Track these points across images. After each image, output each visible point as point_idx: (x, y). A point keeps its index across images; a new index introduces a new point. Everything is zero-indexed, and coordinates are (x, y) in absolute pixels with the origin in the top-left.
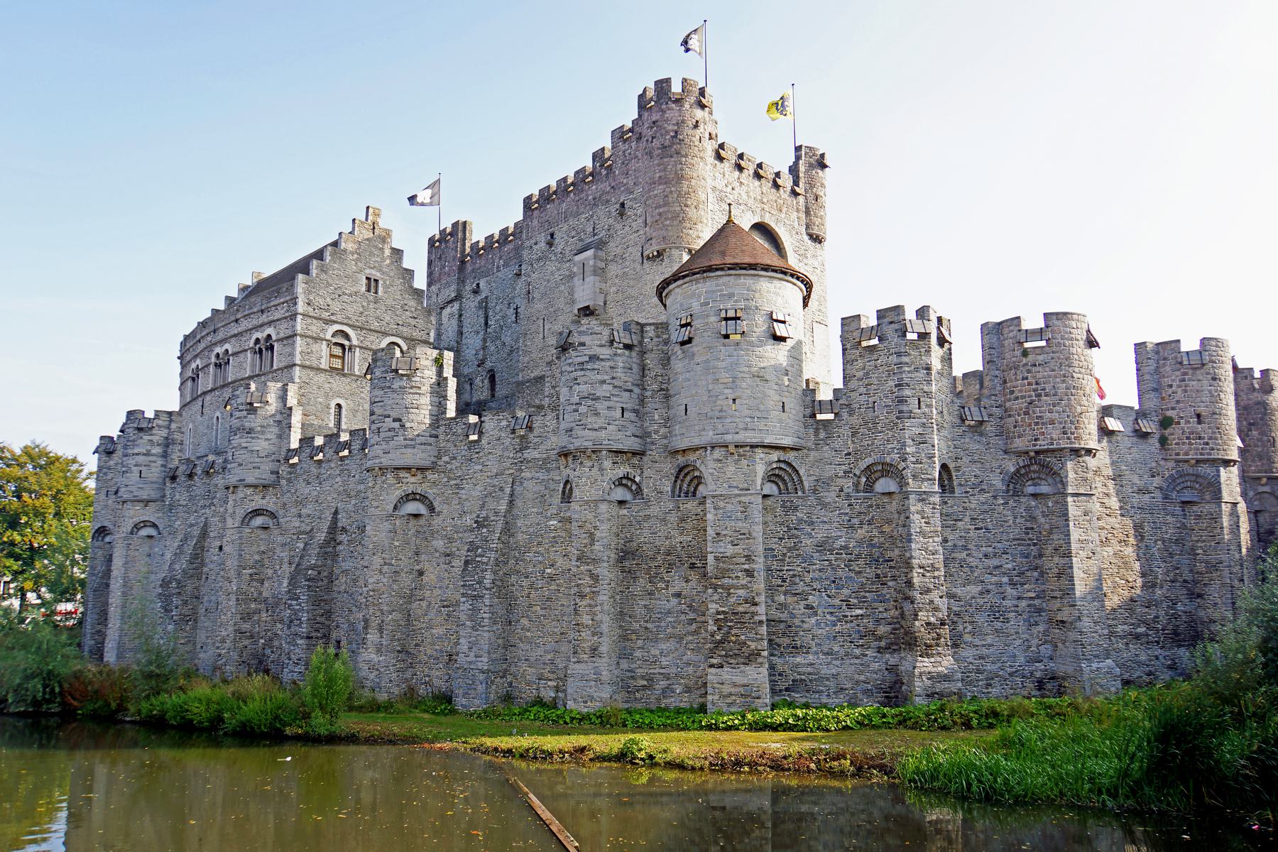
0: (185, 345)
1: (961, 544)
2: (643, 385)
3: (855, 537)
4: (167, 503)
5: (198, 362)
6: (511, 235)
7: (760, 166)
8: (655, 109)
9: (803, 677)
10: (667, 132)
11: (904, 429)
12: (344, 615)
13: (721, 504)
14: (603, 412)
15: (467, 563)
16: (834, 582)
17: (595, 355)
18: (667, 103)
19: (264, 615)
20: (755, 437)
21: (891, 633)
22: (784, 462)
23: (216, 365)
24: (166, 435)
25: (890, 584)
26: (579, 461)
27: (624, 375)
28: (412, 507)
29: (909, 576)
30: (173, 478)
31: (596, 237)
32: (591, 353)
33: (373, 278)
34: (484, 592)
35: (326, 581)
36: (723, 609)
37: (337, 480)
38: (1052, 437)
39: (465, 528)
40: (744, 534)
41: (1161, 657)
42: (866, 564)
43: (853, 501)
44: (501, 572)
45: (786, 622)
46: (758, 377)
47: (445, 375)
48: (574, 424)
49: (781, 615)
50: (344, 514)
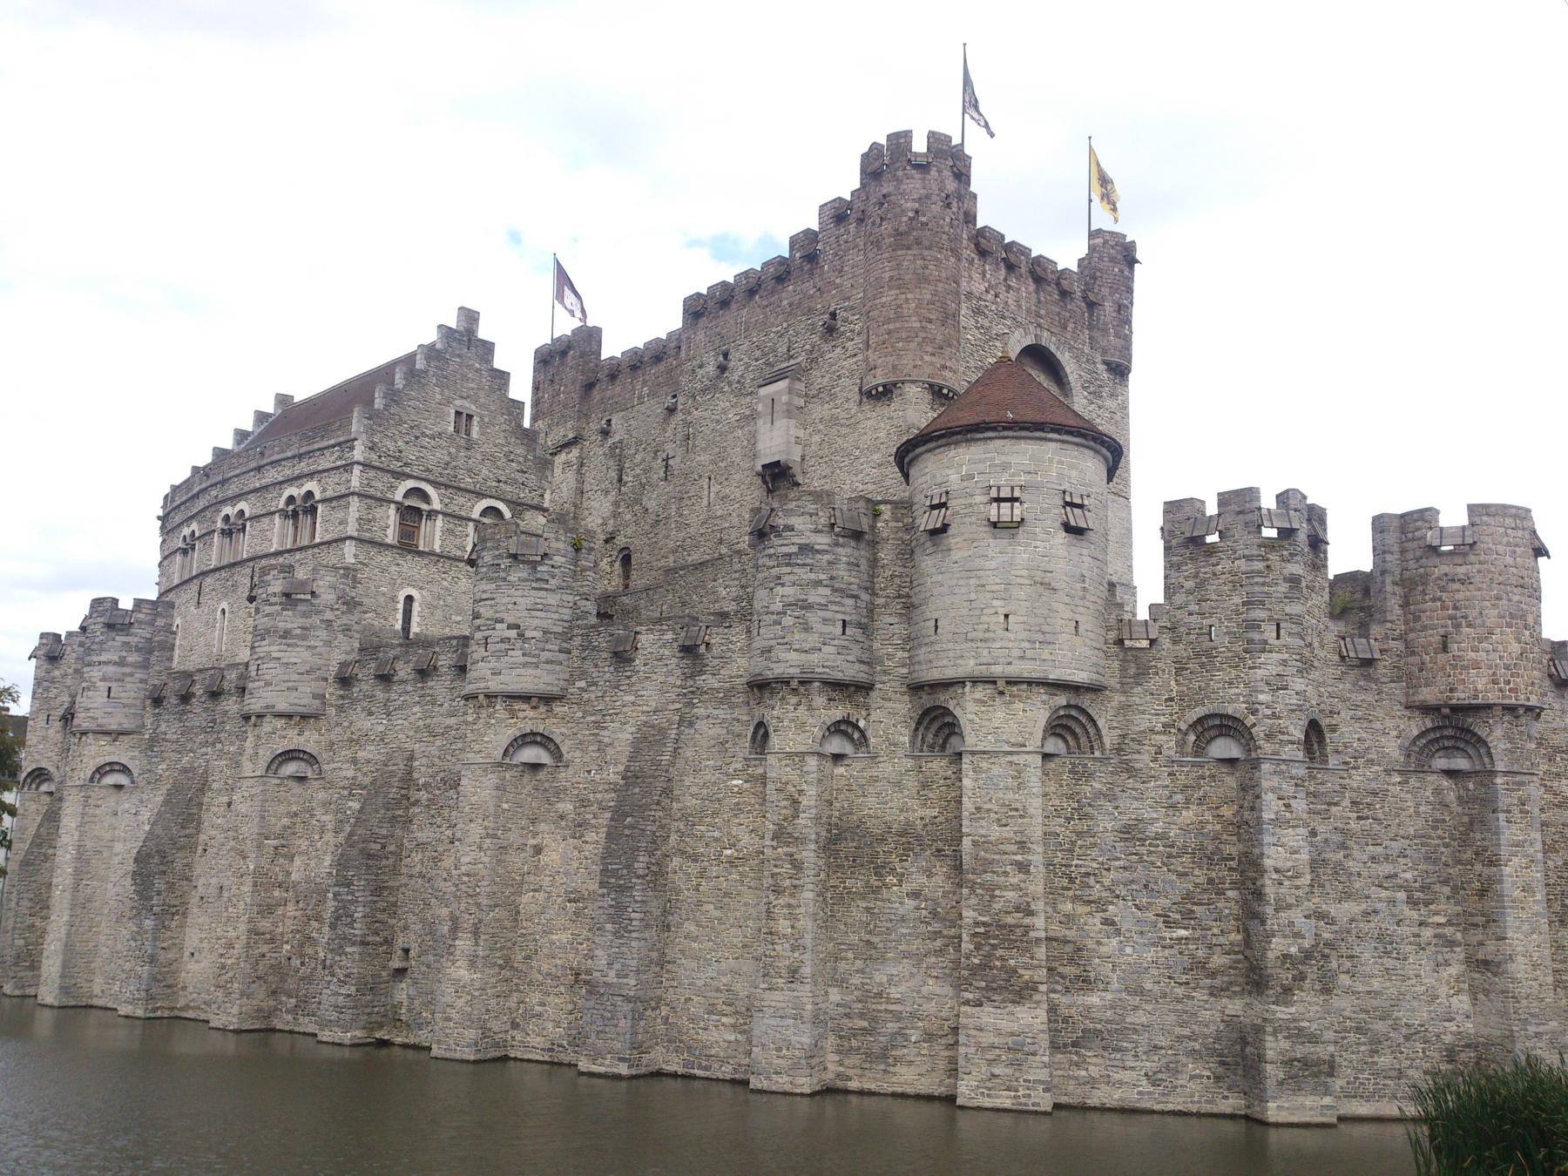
0: (173, 501)
1: (1337, 838)
2: (873, 589)
3: (1179, 821)
4: (147, 736)
5: (194, 526)
8: (887, 176)
9: (1099, 1026)
11: (1255, 668)
12: (417, 911)
13: (984, 765)
14: (818, 627)
15: (609, 836)
16: (1146, 886)
17: (807, 545)
18: (905, 169)
19: (291, 907)
20: (1035, 670)
21: (1230, 968)
22: (1076, 707)
23: (223, 532)
24: (149, 636)
25: (1230, 893)
28: (530, 754)
29: (1258, 883)
30: (157, 701)
31: (792, 362)
32: (803, 541)
33: (465, 412)
34: (633, 880)
35: (391, 861)
36: (984, 919)
37: (415, 710)
38: (1477, 686)
39: (607, 787)
40: (1017, 810)
42: (1193, 862)
43: (1176, 768)
45: (1075, 943)
46: (1042, 584)
49: (1067, 932)
50: (424, 761)
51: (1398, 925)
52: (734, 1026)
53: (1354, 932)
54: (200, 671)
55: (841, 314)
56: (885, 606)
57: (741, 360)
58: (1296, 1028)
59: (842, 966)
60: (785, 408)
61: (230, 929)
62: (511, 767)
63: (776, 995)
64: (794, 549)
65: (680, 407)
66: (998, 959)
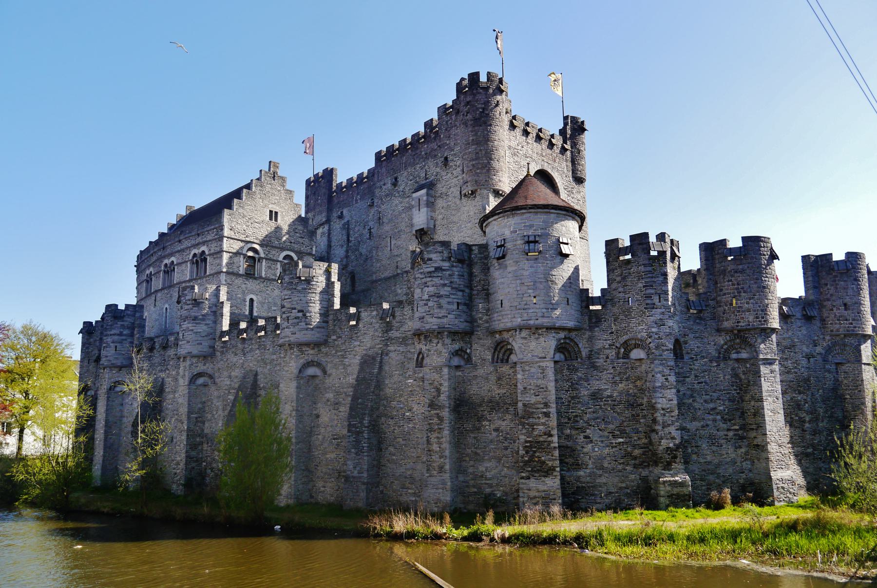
0: (141, 258)
1: (689, 393)
5: (151, 269)
6: (365, 178)
7: (540, 130)
9: (584, 485)
10: (478, 109)
11: (650, 316)
13: (527, 368)
14: (445, 306)
15: (351, 408)
17: (439, 267)
18: (477, 89)
20: (549, 322)
21: (643, 454)
22: (569, 338)
23: (164, 271)
25: (641, 421)
26: (429, 339)
27: (458, 280)
28: (311, 371)
29: (655, 416)
32: (436, 265)
34: (363, 429)
36: (528, 439)
37: (256, 352)
40: (543, 388)
41: (823, 469)
42: (625, 408)
44: (375, 416)
45: (571, 447)
47: (333, 280)
48: (425, 314)
50: (262, 376)
51: (718, 431)
52: (414, 493)
53: (698, 435)
54: (157, 337)
55: (450, 158)
56: (477, 295)
57: (403, 181)
58: (673, 481)
59: (464, 464)
60: (425, 202)
61: (177, 456)
62: (302, 378)
63: (433, 479)
64: (433, 269)
65: (375, 204)
66: (536, 457)
